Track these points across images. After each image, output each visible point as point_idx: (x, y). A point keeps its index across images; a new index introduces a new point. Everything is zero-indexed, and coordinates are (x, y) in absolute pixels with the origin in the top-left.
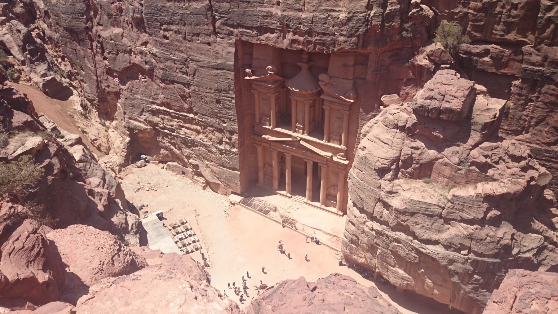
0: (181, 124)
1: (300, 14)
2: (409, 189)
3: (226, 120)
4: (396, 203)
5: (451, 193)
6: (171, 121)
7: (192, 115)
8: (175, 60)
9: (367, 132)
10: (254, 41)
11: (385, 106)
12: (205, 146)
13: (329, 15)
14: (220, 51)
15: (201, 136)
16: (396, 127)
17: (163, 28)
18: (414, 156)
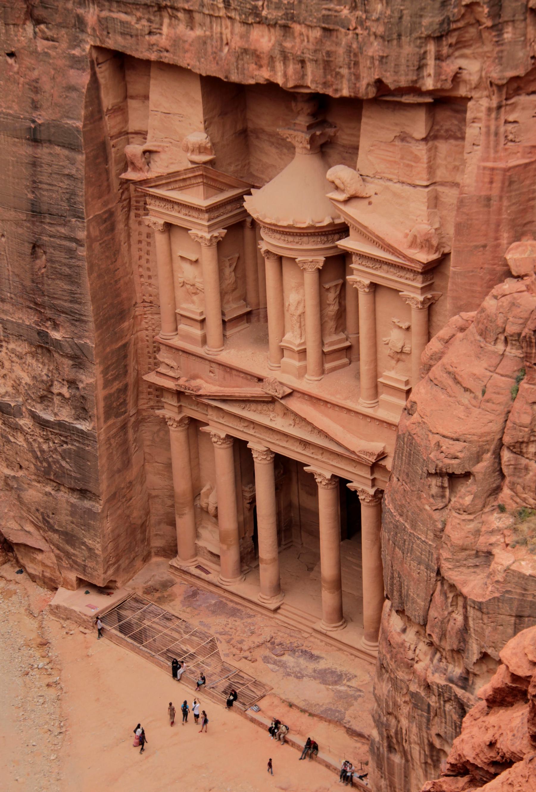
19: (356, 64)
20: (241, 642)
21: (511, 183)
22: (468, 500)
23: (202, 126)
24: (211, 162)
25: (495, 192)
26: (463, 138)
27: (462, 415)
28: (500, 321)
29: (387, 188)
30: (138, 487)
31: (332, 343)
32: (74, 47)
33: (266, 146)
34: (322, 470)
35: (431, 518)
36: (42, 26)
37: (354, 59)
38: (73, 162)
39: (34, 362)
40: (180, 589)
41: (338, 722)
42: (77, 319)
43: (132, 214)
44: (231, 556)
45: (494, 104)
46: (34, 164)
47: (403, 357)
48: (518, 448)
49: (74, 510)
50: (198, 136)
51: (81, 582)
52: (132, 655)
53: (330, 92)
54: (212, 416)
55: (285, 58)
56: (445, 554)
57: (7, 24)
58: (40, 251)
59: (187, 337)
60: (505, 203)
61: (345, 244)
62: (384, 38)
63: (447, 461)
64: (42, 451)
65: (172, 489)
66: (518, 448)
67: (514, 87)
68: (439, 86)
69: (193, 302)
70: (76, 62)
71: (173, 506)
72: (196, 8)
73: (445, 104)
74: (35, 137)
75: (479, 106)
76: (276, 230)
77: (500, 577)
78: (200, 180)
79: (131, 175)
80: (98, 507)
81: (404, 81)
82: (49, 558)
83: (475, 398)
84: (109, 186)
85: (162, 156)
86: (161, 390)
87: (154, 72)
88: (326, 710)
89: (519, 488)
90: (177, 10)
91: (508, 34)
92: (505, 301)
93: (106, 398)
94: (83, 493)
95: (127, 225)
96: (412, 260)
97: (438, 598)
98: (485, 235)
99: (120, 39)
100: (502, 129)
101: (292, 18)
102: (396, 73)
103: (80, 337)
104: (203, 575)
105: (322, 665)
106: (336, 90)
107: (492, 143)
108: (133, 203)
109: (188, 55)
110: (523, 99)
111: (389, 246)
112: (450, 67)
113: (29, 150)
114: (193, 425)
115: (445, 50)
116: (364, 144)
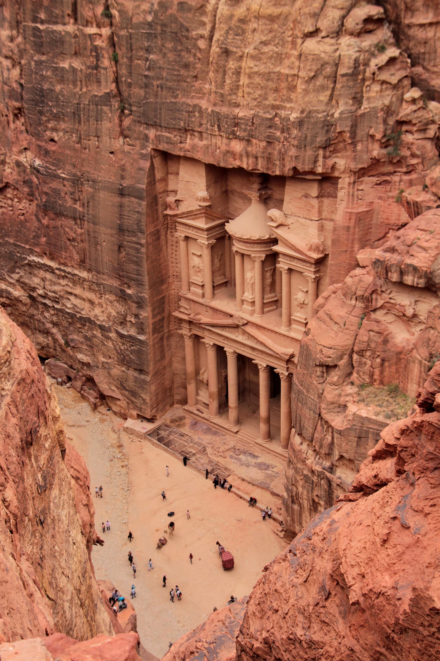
0: (70, 290)
1: (237, 110)
6: (55, 284)
7: (84, 274)
8: (64, 179)
12: (101, 328)
13: (276, 115)
17: (50, 126)
19: (283, 159)
20: (219, 448)
21: (360, 220)
22: (335, 378)
23: (205, 188)
24: (209, 206)
25: (352, 224)
26: (336, 197)
27: (333, 336)
28: (353, 289)
29: (298, 221)
30: (168, 369)
31: (268, 298)
32: (143, 149)
33: (237, 199)
34: (262, 362)
35: (316, 387)
36: (128, 139)
37: (282, 157)
38: (140, 205)
39: (118, 305)
40: (188, 421)
41: (267, 489)
42: (140, 284)
43: (169, 231)
44: (214, 405)
45: (352, 181)
46: (121, 206)
47: (304, 306)
48: (361, 353)
49: (136, 380)
50: (203, 193)
51: (139, 416)
52: (164, 453)
53: (270, 173)
54: (206, 334)
55: (248, 155)
56: (323, 406)
57: (110, 138)
58: (122, 249)
59: (195, 294)
60: (357, 230)
61: (276, 248)
62: (298, 147)
63: (326, 359)
64: (121, 350)
65: (185, 370)
66: (361, 353)
67: (361, 173)
68: (324, 171)
69: (198, 276)
70: (143, 156)
71: (186, 379)
72: (204, 130)
73: (328, 180)
74: (122, 193)
75: (345, 181)
76: (241, 240)
77: (350, 418)
78: (203, 215)
79: (169, 212)
80: (148, 379)
81: (307, 168)
82: (123, 403)
83: (340, 327)
84: (157, 217)
85: (185, 203)
86: (181, 320)
87: (182, 162)
88: (261, 483)
89: (361, 373)
90: (194, 131)
91: (359, 147)
92: (356, 279)
93: (153, 324)
94: (141, 371)
95: (166, 237)
96: (310, 257)
97: (319, 428)
98: (347, 245)
99: (165, 145)
100: (356, 193)
101: (252, 136)
102: (303, 164)
103: (141, 293)
104: (200, 414)
105: (259, 460)
106: (273, 172)
107: (351, 200)
108: (169, 226)
109: (199, 153)
110: (366, 179)
111: (298, 250)
112: (330, 162)
113: (119, 199)
114: (197, 338)
115: (328, 154)
116: (287, 198)
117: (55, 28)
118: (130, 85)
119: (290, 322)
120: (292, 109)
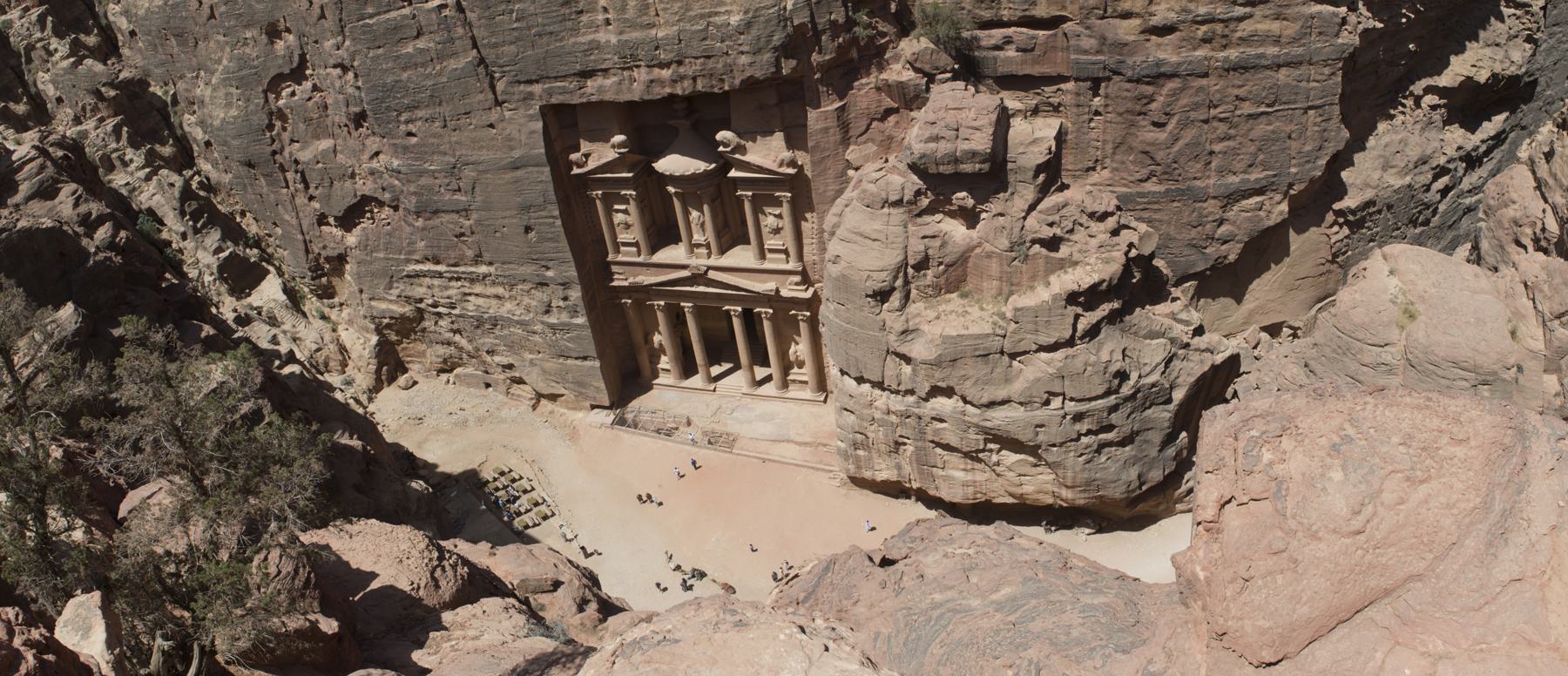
1: (654, 32)
2: (938, 318)
3: (550, 264)
4: (919, 349)
5: (1010, 306)
7: (483, 269)
9: (837, 226)
10: (576, 100)
11: (857, 169)
12: (521, 323)
14: (515, 134)
15: (508, 305)
16: (886, 203)
18: (930, 252)
79: (576, 171)
117: (387, 16)
118: (495, 46)
119: (762, 255)
120: (728, 12)
